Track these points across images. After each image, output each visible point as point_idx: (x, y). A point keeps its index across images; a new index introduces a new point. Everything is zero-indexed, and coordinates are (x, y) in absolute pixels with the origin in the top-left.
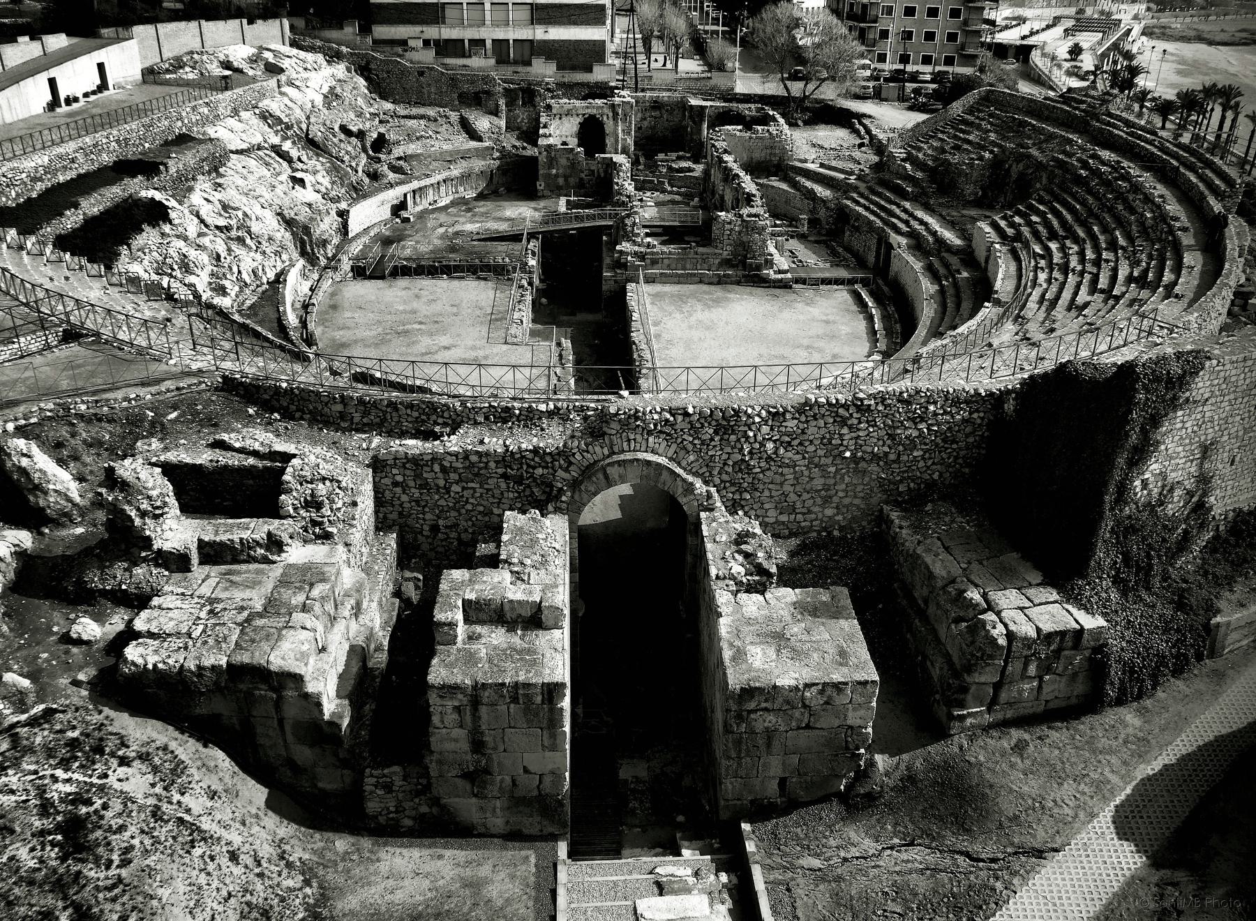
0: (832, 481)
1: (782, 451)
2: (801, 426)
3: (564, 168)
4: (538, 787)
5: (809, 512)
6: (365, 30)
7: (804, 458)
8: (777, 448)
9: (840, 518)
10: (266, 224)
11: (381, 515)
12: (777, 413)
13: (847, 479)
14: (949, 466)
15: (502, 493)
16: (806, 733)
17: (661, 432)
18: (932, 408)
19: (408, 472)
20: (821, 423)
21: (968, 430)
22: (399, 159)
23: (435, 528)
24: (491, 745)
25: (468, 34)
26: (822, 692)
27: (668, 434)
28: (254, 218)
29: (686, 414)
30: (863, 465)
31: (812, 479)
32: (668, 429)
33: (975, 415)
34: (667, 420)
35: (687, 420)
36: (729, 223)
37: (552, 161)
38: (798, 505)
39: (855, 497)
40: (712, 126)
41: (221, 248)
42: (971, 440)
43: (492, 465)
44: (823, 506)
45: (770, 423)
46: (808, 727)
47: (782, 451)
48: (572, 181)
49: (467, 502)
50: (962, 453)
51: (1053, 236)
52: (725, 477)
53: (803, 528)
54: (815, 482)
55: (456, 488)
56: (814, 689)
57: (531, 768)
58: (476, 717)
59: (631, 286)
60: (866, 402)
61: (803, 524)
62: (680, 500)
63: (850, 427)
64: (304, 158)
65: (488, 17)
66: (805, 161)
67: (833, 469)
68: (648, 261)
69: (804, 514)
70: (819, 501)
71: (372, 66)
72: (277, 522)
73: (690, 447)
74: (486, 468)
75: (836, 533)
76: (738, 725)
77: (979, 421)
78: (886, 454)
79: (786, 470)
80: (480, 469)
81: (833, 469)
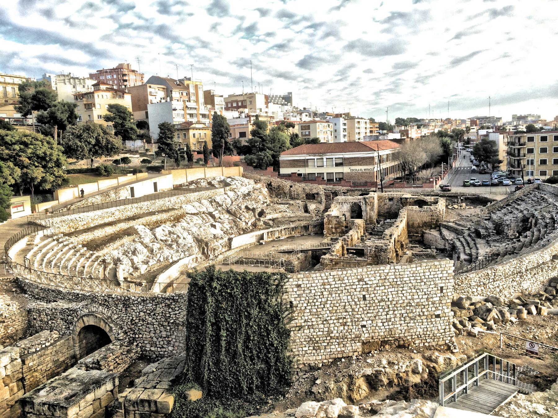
1: (147, 317)
5: (163, 347)
9: (174, 352)
13: (175, 334)
25: (316, 171)
27: (107, 306)
28: (182, 238)
31: (161, 332)
32: (107, 303)
34: (106, 300)
36: (370, 247)
37: (329, 222)
43: (58, 314)
45: (142, 304)
48: (339, 230)
53: (161, 355)
61: (161, 353)
65: (325, 164)
66: (450, 222)
67: (168, 328)
68: (334, 263)
71: (272, 184)
74: (57, 315)
79: (150, 326)
81: (168, 328)
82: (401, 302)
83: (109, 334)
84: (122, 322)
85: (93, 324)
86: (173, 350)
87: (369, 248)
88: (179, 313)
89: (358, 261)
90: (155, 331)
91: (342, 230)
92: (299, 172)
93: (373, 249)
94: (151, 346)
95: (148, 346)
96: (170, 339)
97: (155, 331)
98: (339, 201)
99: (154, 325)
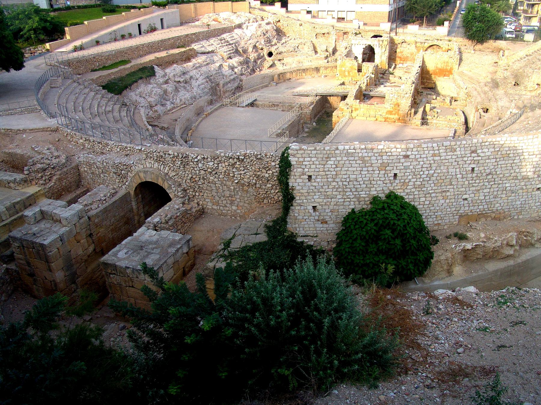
9: (239, 211)
13: (240, 194)
30: (246, 188)
34: (162, 156)
45: (202, 162)
53: (224, 213)
54: (225, 192)
61: (223, 211)
74: (109, 168)
75: (238, 218)
81: (232, 188)
82: (508, 175)
84: (180, 180)
86: (238, 209)
88: (245, 173)
90: (217, 190)
92: (308, 10)
94: (213, 205)
95: (209, 204)
96: (234, 199)
97: (217, 190)
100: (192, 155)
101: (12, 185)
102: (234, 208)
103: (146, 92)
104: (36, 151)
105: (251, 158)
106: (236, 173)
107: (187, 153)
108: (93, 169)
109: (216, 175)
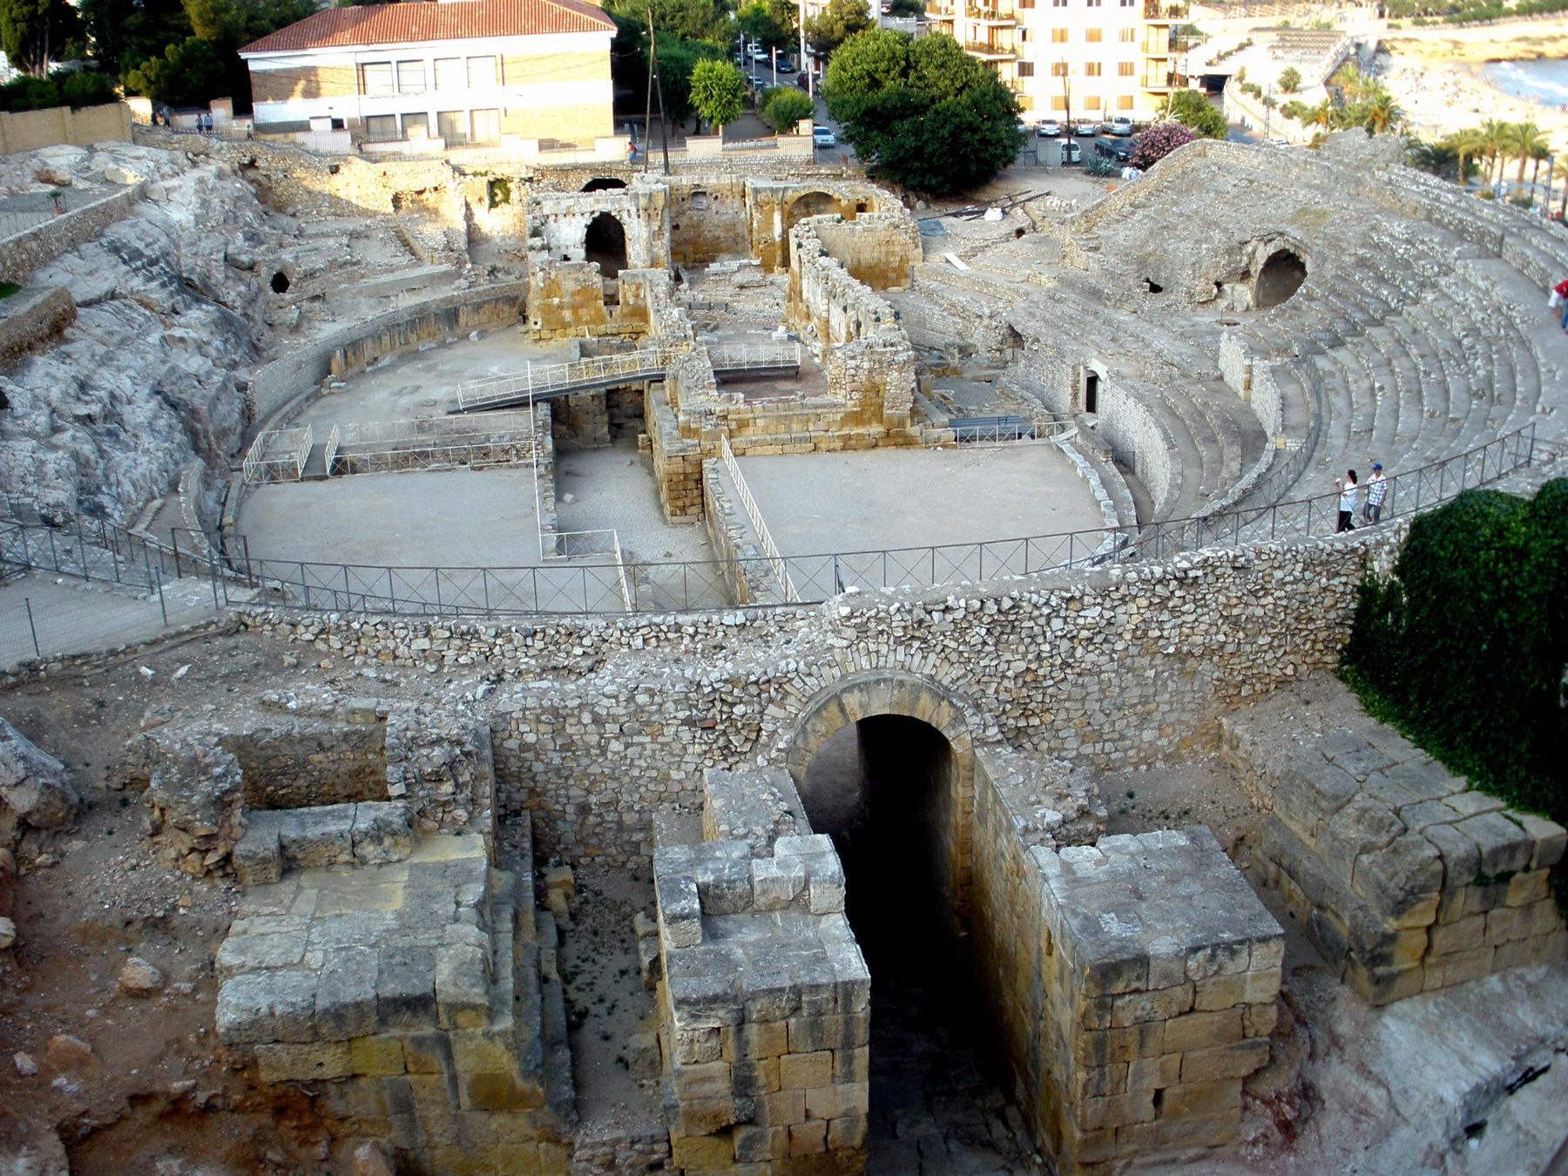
0: (1152, 690)
2: (1107, 614)
3: (573, 294)
4: (825, 1138)
5: (1123, 737)
6: (243, 108)
7: (1112, 660)
8: (1074, 649)
10: (142, 409)
11: (503, 796)
12: (1072, 598)
13: (1171, 686)
14: (1307, 654)
15: (685, 748)
16: (1192, 1020)
17: (913, 637)
18: (1279, 574)
19: (542, 728)
20: (1132, 608)
21: (1329, 601)
22: (315, 298)
23: (584, 809)
24: (762, 1081)
25: (397, 107)
26: (1213, 957)
29: (947, 610)
31: (1123, 690)
33: (1336, 581)
35: (949, 617)
38: (1106, 729)
39: (1183, 710)
40: (789, 220)
41: (87, 449)
42: (1332, 615)
43: (670, 706)
44: (1140, 727)
45: (1063, 613)
46: (1192, 1010)
47: (1079, 652)
49: (632, 765)
50: (1322, 636)
51: (1337, 343)
52: (1003, 696)
55: (615, 746)
56: (1200, 955)
57: (816, 1112)
58: (742, 1044)
59: (707, 464)
60: (1191, 574)
61: (1113, 756)
62: (945, 733)
63: (1172, 610)
64: (180, 307)
68: (733, 426)
69: (1113, 741)
70: (1134, 720)
71: (259, 163)
72: (385, 805)
73: (954, 657)
74: (659, 711)
75: (1160, 764)
76: (1101, 1018)
77: (1341, 588)
78: (1222, 645)
80: (651, 714)
81: (1152, 673)
83: (949, 734)
85: (887, 711)
86: (1160, 738)
87: (852, 363)
89: (816, 407)
91: (598, 310)
92: (335, 116)
93: (866, 365)
98: (546, 211)
99: (1102, 672)
100: (1035, 598)
101: (369, 849)
102: (1148, 735)
103: (19, 472)
104: (297, 713)
105: (1218, 572)
106: (1167, 626)
107: (1015, 594)
108: (570, 730)
109: (1105, 646)
